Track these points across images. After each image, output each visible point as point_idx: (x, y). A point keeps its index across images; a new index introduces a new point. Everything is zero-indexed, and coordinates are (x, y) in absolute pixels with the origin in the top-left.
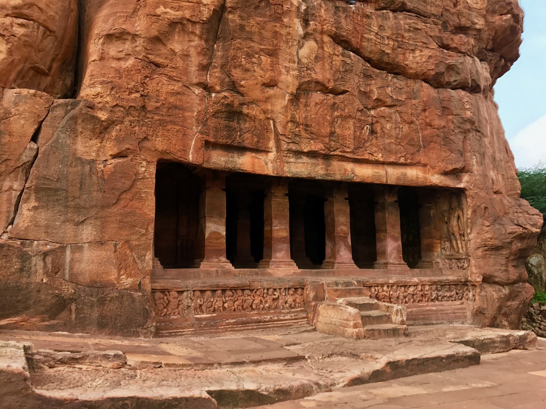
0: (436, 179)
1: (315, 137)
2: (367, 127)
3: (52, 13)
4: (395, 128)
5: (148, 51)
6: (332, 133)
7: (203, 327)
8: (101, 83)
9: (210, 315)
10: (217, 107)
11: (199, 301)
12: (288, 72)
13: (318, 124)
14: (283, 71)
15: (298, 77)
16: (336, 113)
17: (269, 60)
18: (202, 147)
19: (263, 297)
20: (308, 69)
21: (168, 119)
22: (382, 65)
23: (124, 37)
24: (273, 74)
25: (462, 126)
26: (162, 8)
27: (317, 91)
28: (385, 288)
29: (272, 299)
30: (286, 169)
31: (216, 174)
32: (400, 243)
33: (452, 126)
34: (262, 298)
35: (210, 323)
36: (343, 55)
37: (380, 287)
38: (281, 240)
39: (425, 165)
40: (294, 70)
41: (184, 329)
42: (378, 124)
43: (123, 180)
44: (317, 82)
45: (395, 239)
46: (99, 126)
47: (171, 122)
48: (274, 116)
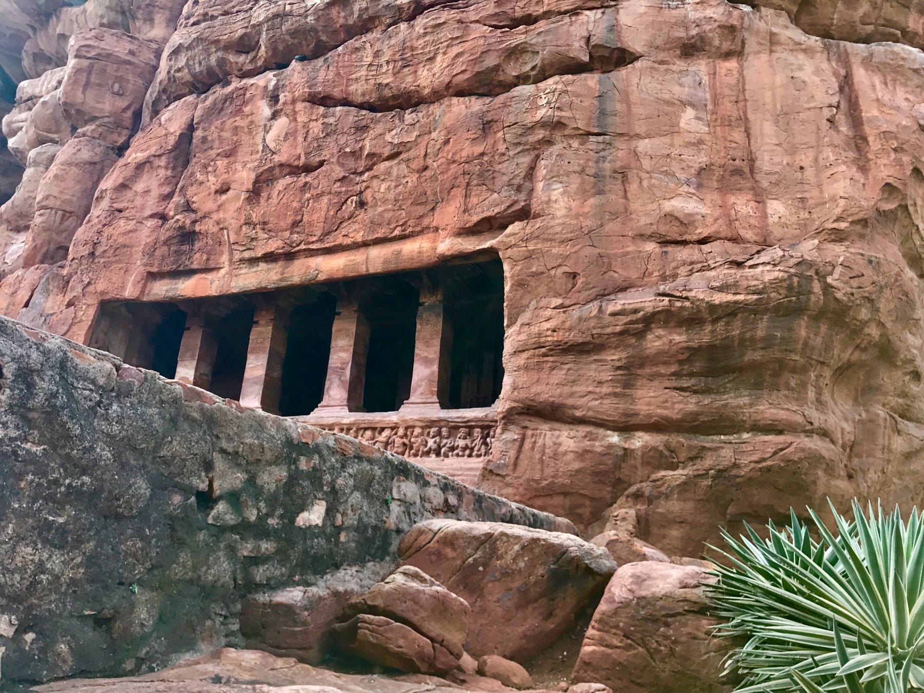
0: (446, 245)
1: (274, 234)
3: (68, 197)
4: (396, 187)
6: (296, 224)
10: (168, 234)
16: (308, 195)
20: (274, 153)
21: (114, 259)
22: (391, 103)
25: (524, 139)
30: (233, 284)
32: (435, 368)
38: (255, 381)
45: (427, 362)
47: (116, 262)
48: (226, 224)
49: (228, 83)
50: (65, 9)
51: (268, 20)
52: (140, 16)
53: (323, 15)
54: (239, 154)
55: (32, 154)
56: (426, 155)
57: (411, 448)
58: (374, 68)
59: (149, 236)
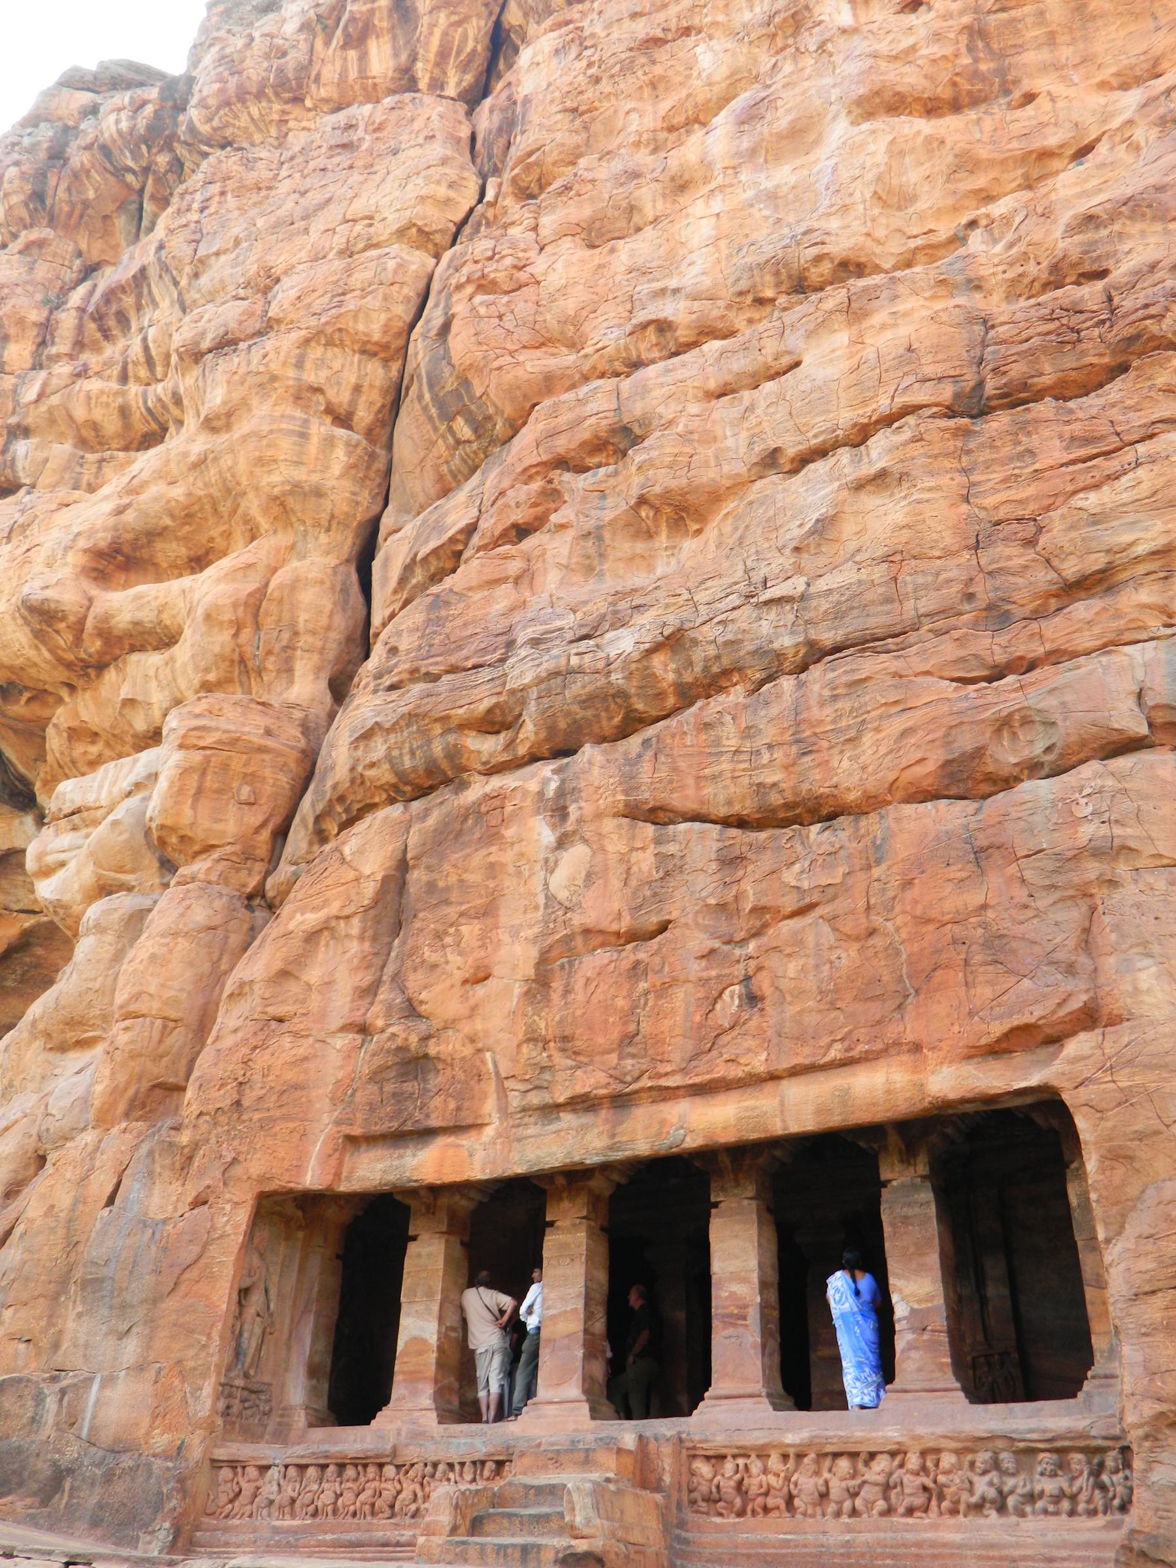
2: (733, 993)
3: (173, 993)
6: (629, 1039)
10: (378, 1061)
11: (289, 1489)
13: (590, 1028)
16: (643, 985)
18: (336, 1150)
19: (422, 1484)
20: (568, 909)
24: (482, 954)
25: (1060, 880)
26: (299, 917)
27: (594, 950)
28: (774, 1462)
30: (515, 1156)
33: (1021, 894)
34: (418, 1487)
36: (658, 841)
37: (753, 1457)
39: (917, 1048)
42: (764, 973)
44: (587, 932)
49: (464, 786)
50: (135, 657)
51: (539, 681)
52: (270, 667)
53: (637, 669)
54: (502, 912)
55: (94, 911)
56: (868, 908)
57: (941, 1497)
58: (745, 757)
59: (341, 1067)
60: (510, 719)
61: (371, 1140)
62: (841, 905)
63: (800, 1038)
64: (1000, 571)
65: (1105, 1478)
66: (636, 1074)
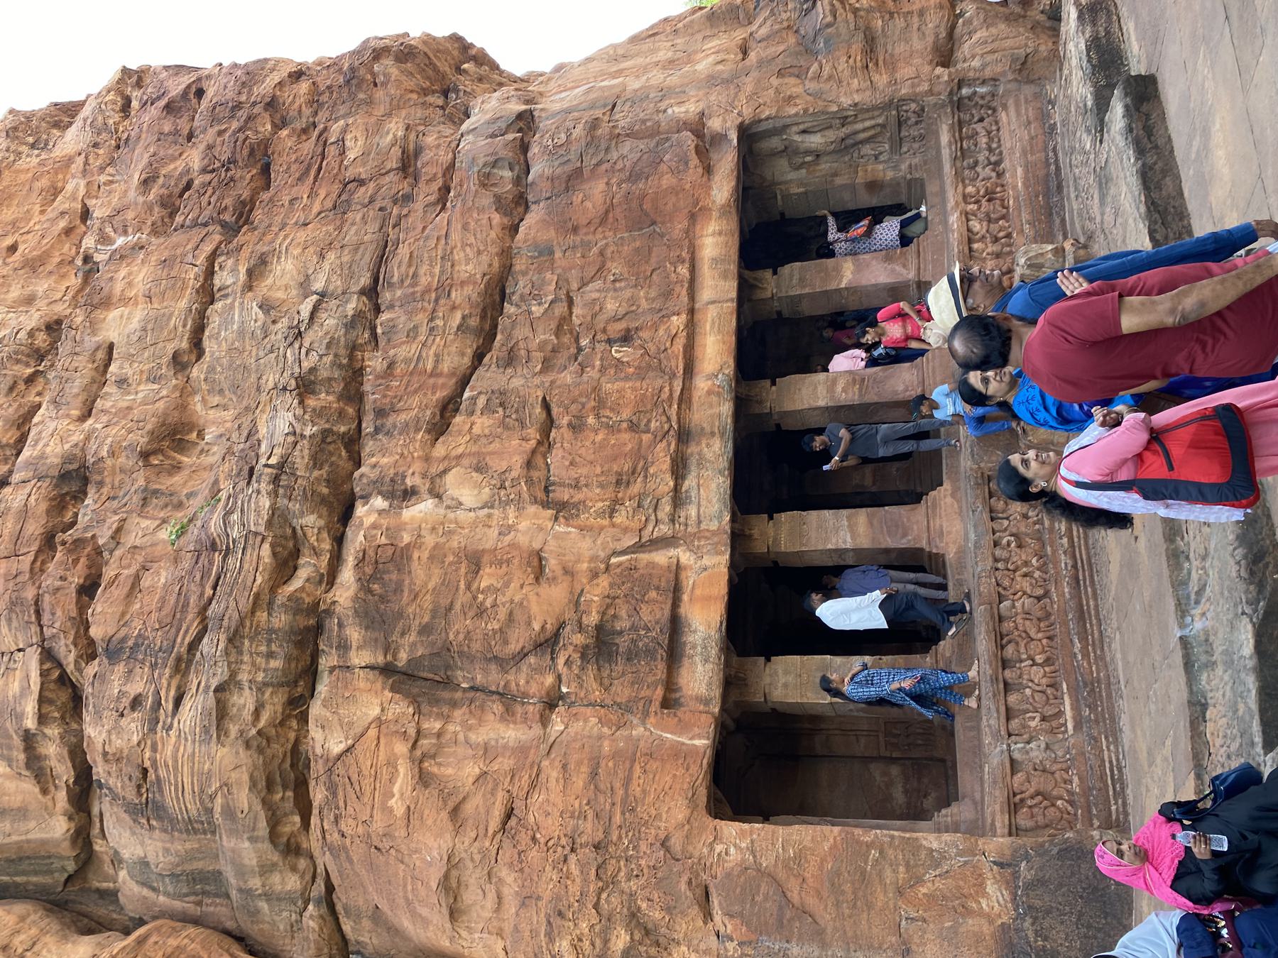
2: (617, 351)
5: (481, 835)
6: (633, 427)
7: (1096, 716)
8: (551, 940)
9: (1066, 697)
11: (1033, 724)
12: (510, 528)
14: (508, 539)
15: (520, 505)
16: (591, 420)
17: (487, 570)
18: (675, 715)
19: (1015, 571)
20: (503, 487)
22: (487, 327)
23: (454, 885)
26: (392, 802)
29: (1018, 550)
30: (714, 526)
31: (732, 683)
33: (605, 166)
35: (1085, 699)
36: (472, 413)
40: (506, 518)
41: (1103, 761)
43: (759, 898)
44: (529, 464)
46: (642, 949)
48: (602, 554)
51: (274, 494)
60: (291, 544)
61: (670, 685)
62: (574, 276)
63: (667, 294)
64: (371, 197)
65: (976, 119)
66: (664, 418)
